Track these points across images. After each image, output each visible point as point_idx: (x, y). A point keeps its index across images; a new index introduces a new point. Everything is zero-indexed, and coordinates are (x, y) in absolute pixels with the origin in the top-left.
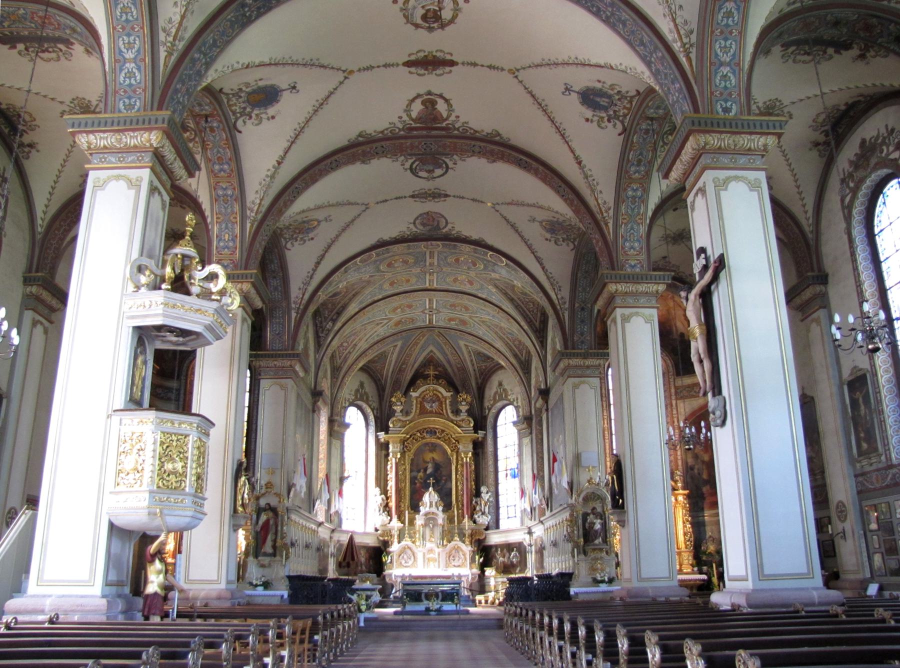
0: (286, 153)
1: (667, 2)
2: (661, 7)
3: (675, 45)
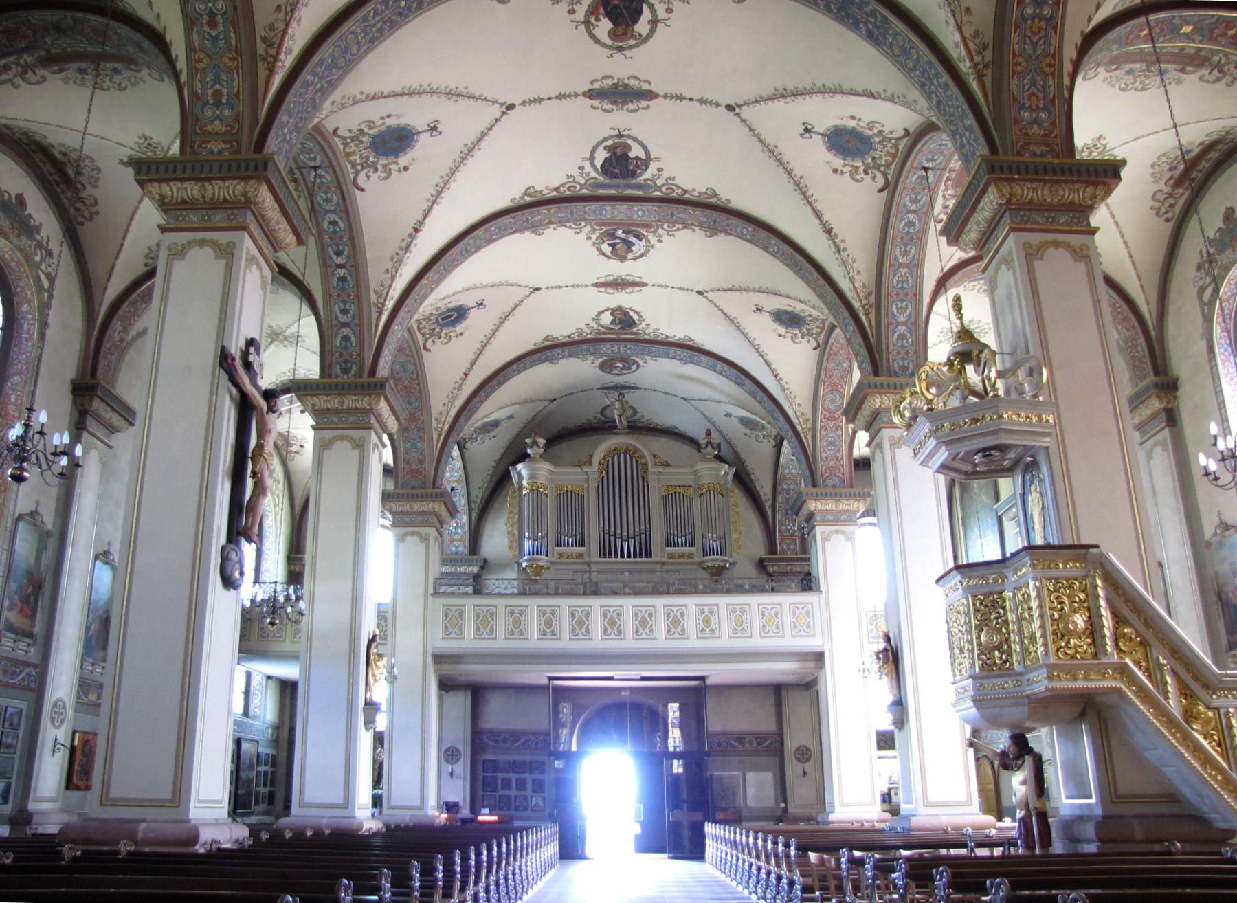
0: (473, 364)
1: (950, 4)
2: (942, 11)
3: (961, 65)
